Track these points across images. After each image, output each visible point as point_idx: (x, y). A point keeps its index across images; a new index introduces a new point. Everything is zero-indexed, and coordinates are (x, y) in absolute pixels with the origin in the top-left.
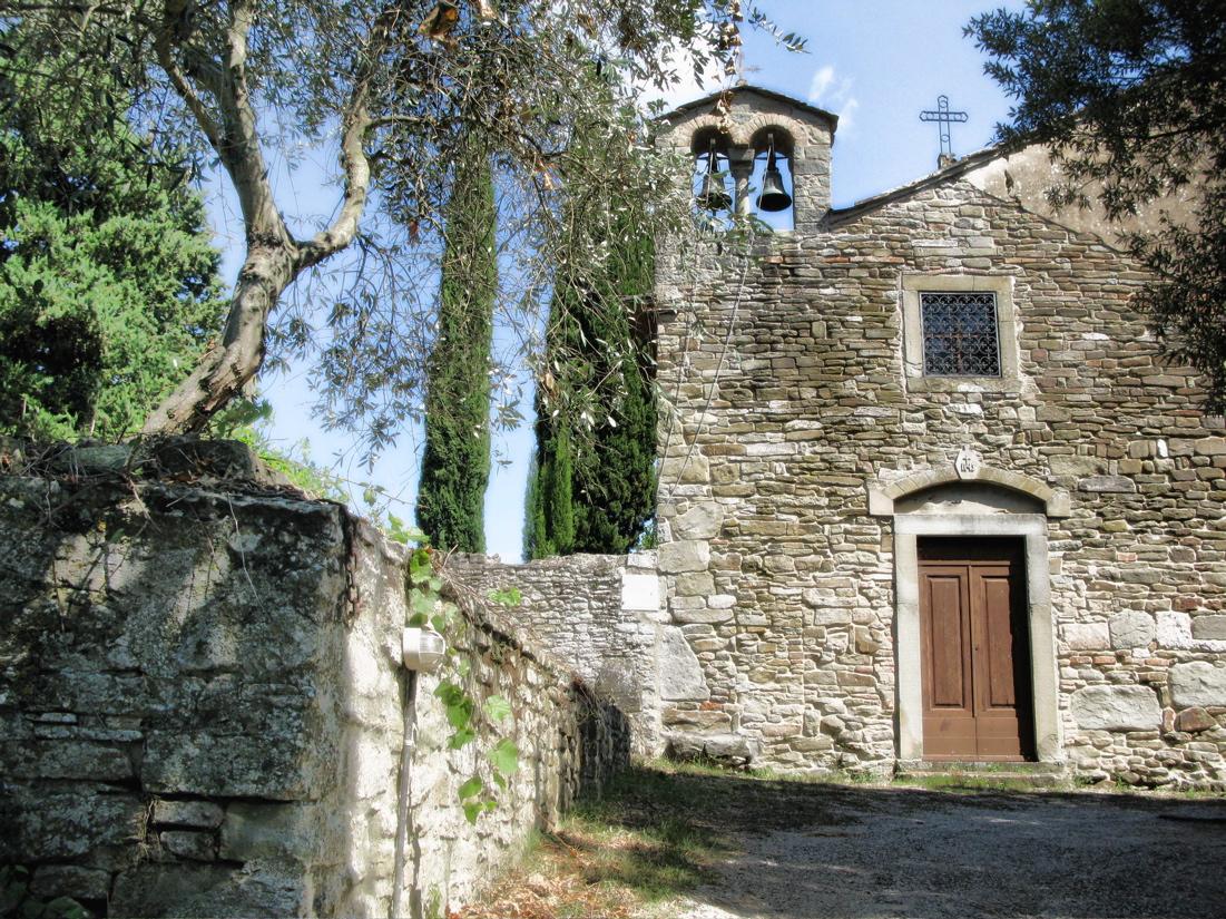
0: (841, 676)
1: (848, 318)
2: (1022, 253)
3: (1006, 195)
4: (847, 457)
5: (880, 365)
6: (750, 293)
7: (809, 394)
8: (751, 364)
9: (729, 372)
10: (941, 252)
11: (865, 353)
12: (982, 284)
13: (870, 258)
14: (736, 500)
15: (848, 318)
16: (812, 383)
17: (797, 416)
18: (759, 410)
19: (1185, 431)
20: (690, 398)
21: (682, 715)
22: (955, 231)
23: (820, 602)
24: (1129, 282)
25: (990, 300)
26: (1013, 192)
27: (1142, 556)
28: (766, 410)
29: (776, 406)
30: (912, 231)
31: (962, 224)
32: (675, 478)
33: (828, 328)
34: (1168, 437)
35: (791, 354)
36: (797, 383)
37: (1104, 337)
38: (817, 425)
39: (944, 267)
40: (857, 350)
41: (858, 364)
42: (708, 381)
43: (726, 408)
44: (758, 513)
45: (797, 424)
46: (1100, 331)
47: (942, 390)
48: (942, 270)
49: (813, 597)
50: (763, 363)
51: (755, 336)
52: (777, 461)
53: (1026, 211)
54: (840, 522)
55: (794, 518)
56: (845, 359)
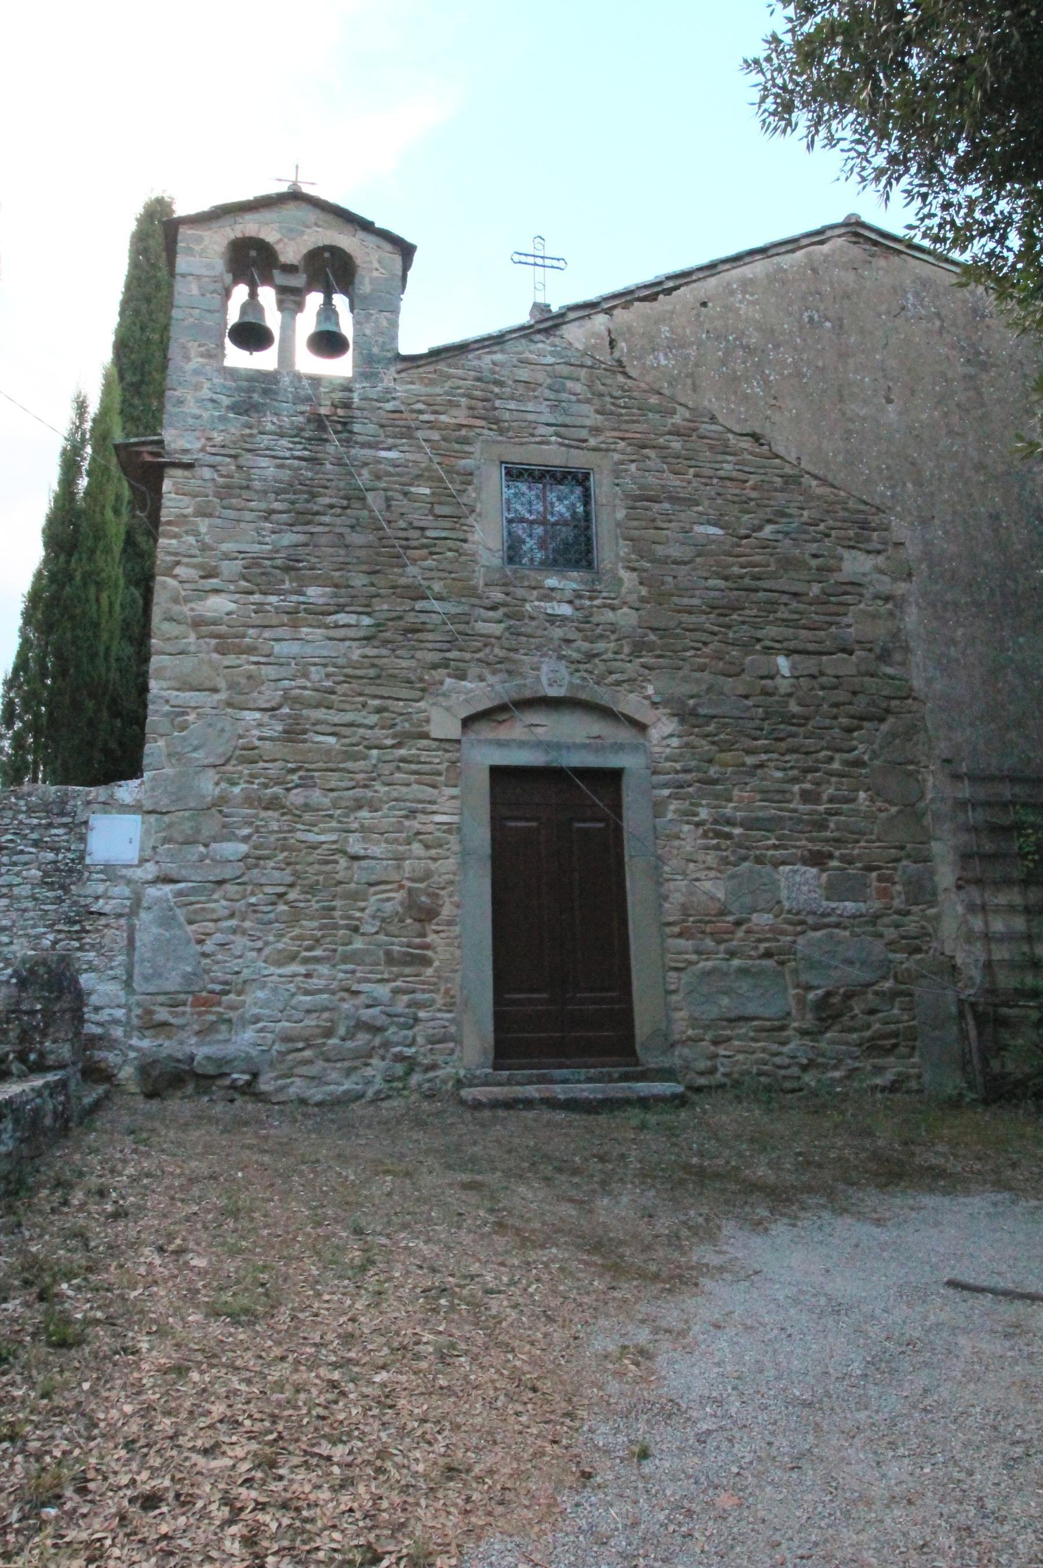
0: (388, 953)
1: (413, 489)
2: (625, 426)
3: (608, 357)
4: (404, 664)
5: (450, 550)
6: (290, 449)
7: (359, 580)
8: (288, 538)
9: (257, 547)
10: (531, 417)
11: (429, 533)
12: (578, 459)
13: (443, 418)
14: (257, 715)
15: (413, 489)
16: (365, 568)
17: (340, 609)
18: (294, 598)
19: (811, 647)
20: (202, 577)
21: (162, 1014)
22: (548, 393)
23: (362, 853)
24: (747, 469)
25: (586, 476)
26: (617, 354)
27: (766, 796)
28: (302, 599)
29: (315, 594)
30: (496, 390)
31: (557, 387)
32: (173, 683)
33: (388, 499)
34: (789, 653)
35: (338, 530)
36: (342, 567)
37: (720, 532)
38: (366, 621)
39: (533, 435)
40: (423, 529)
41: (423, 546)
42: (227, 557)
43: (252, 593)
44: (285, 732)
45: (342, 618)
46: (715, 525)
47: (526, 584)
48: (533, 440)
49: (355, 846)
50: (302, 538)
51: (292, 503)
52: (315, 664)
53: (630, 377)
54: (393, 747)
55: (332, 740)
56: (407, 539)
